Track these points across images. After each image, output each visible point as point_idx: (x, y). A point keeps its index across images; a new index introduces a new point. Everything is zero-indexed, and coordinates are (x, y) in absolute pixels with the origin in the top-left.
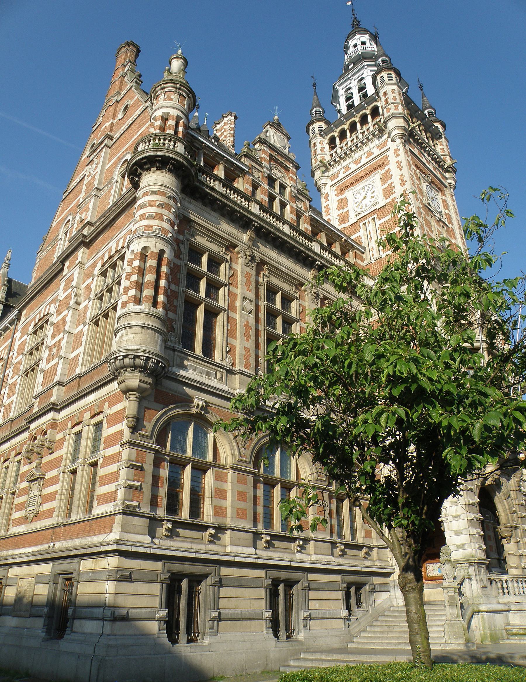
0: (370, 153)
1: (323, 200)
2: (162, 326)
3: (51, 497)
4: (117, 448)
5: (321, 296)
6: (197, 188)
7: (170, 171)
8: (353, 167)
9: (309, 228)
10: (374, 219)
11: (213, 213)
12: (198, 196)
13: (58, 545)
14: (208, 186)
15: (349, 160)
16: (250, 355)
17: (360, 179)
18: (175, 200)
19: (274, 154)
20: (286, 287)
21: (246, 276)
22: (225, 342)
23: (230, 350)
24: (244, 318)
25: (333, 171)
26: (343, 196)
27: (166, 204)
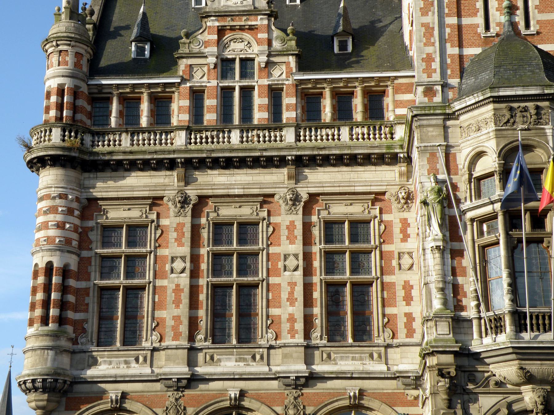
2: (53, 341)
5: (305, 197)
6: (95, 161)
7: (51, 166)
9: (293, 100)
11: (126, 174)
12: (100, 167)
14: (104, 154)
16: (181, 323)
18: (61, 196)
19: (228, 22)
20: (246, 212)
21: (176, 230)
22: (150, 319)
23: (158, 325)
24: (173, 282)
27: (50, 207)
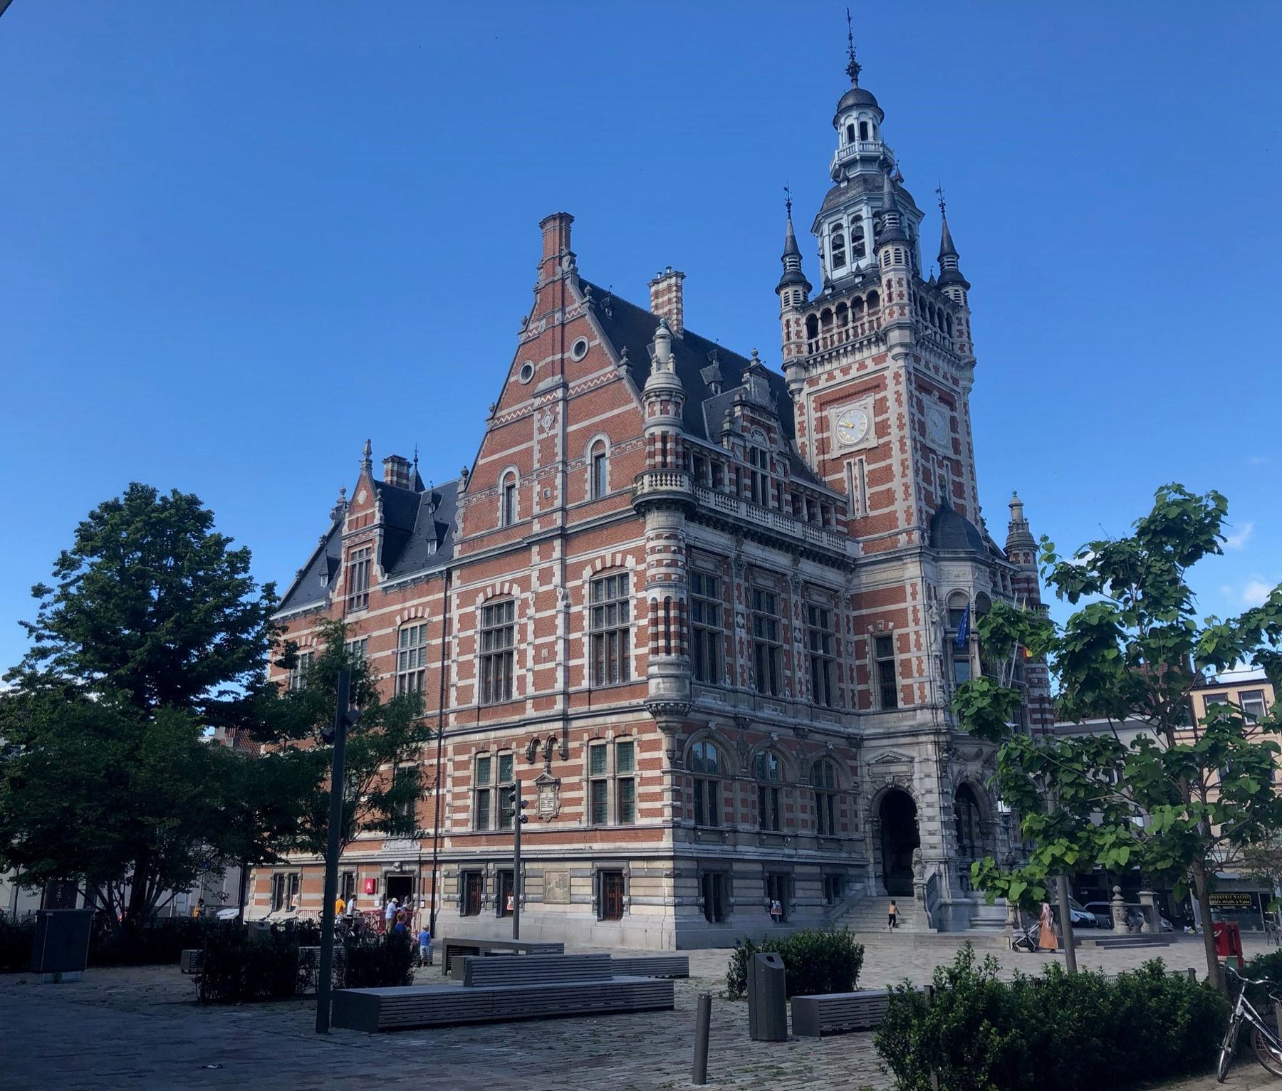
0: (862, 366)
1: (797, 412)
3: (577, 802)
4: (657, 773)
8: (839, 377)
10: (861, 461)
13: (596, 846)
15: (835, 364)
17: (849, 396)
25: (814, 372)
26: (824, 414)
